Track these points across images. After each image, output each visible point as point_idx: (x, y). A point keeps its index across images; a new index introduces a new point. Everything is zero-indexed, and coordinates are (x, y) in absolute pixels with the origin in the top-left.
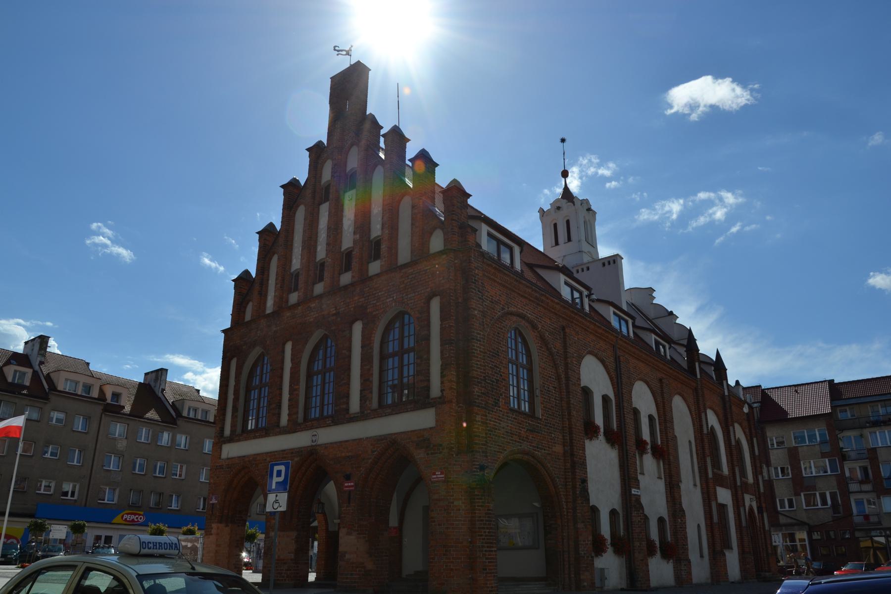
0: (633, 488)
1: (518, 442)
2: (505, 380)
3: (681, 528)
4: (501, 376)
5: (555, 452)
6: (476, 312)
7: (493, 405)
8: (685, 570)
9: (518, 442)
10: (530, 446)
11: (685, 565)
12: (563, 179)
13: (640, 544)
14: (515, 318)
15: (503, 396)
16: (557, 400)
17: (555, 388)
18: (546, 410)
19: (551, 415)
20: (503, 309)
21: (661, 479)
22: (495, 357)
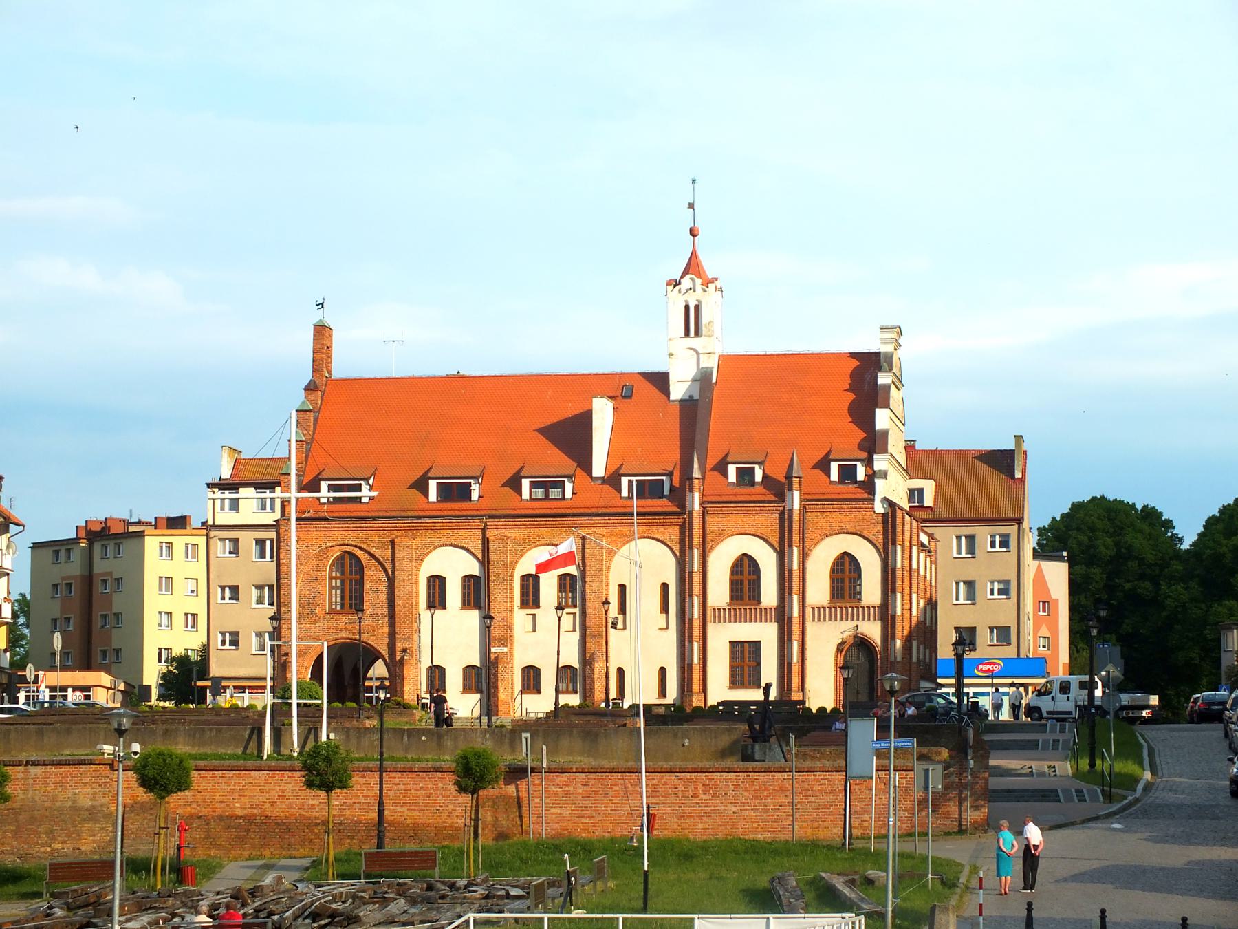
12: (692, 238)
20: (319, 547)
21: (574, 630)
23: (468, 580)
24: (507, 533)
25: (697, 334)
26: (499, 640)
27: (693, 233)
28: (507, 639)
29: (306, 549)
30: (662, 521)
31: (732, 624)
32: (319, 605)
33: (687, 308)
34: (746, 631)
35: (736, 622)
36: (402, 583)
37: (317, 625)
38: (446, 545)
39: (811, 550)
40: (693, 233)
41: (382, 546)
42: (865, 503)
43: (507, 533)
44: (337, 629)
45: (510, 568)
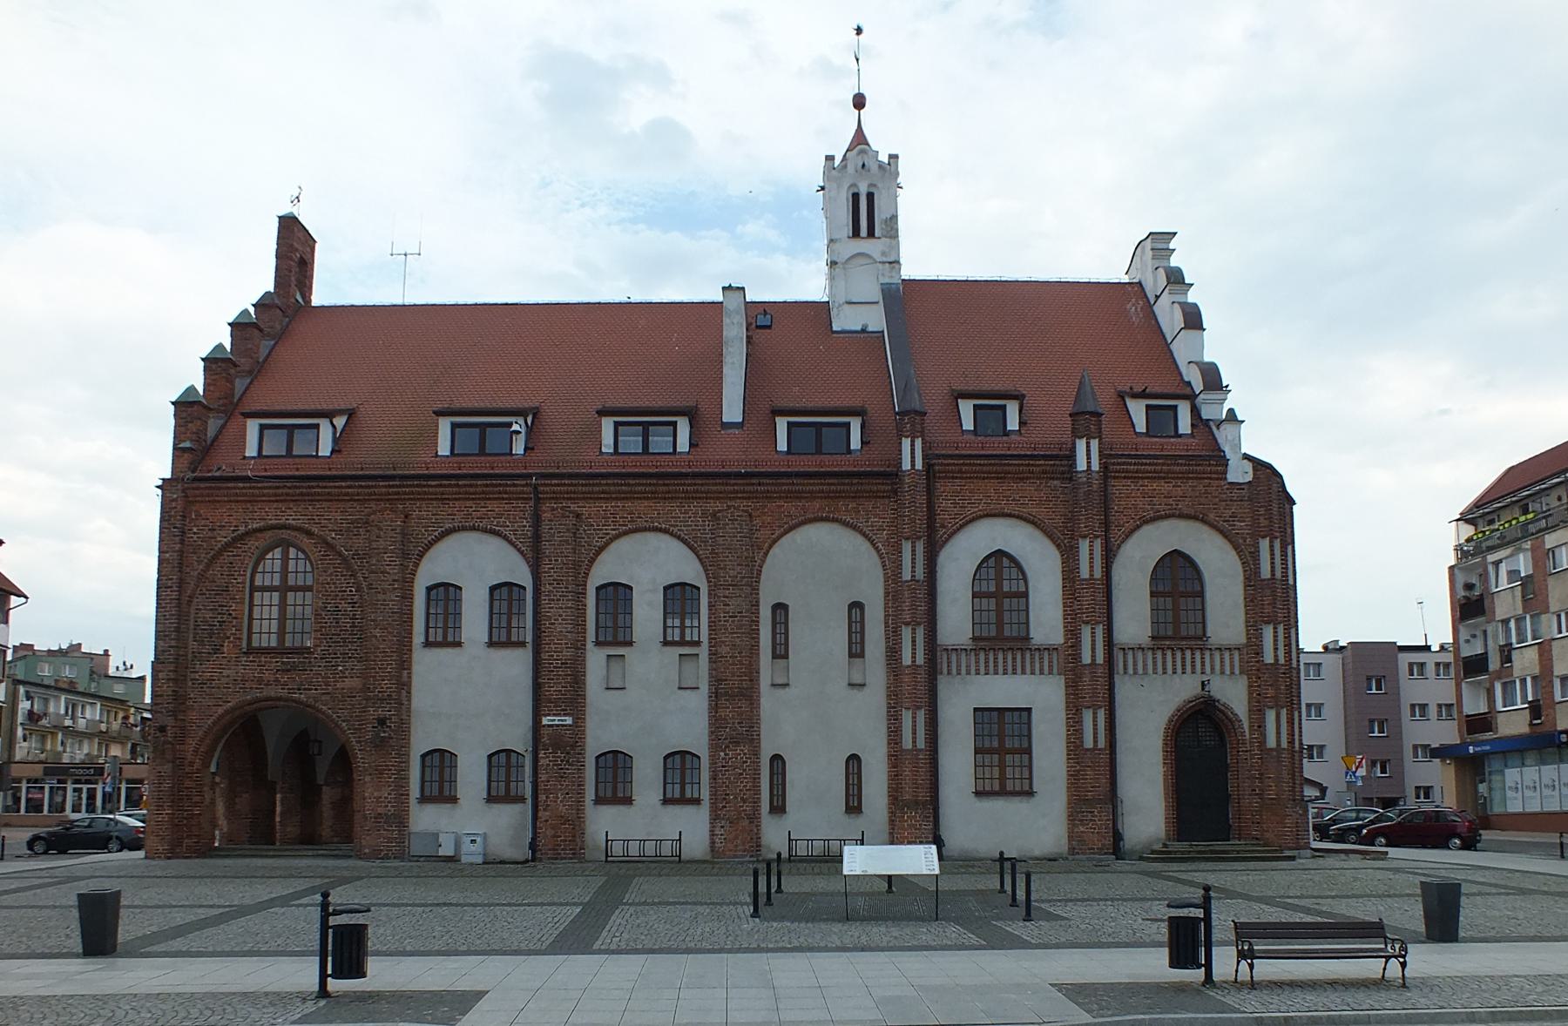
0: (549, 715)
1: (257, 688)
2: (235, 618)
3: (723, 767)
4: (230, 614)
5: (343, 689)
6: (167, 555)
7: (209, 653)
8: (721, 835)
9: (257, 688)
10: (282, 689)
11: (722, 827)
12: (857, 112)
13: (547, 797)
14: (269, 533)
15: (232, 639)
16: (357, 619)
17: (355, 603)
18: (326, 639)
19: (339, 642)
22: (222, 595)
23: (503, 593)
24: (573, 507)
25: (871, 234)
26: (556, 702)
27: (859, 102)
28: (575, 702)
29: (210, 534)
30: (854, 488)
31: (982, 678)
32: (229, 638)
33: (856, 197)
34: (1003, 690)
35: (997, 674)
36: (380, 597)
37: (225, 673)
38: (464, 529)
39: (1119, 546)
40: (859, 102)
41: (348, 529)
42: (1212, 462)
43: (573, 507)
44: (260, 681)
45: (580, 572)
